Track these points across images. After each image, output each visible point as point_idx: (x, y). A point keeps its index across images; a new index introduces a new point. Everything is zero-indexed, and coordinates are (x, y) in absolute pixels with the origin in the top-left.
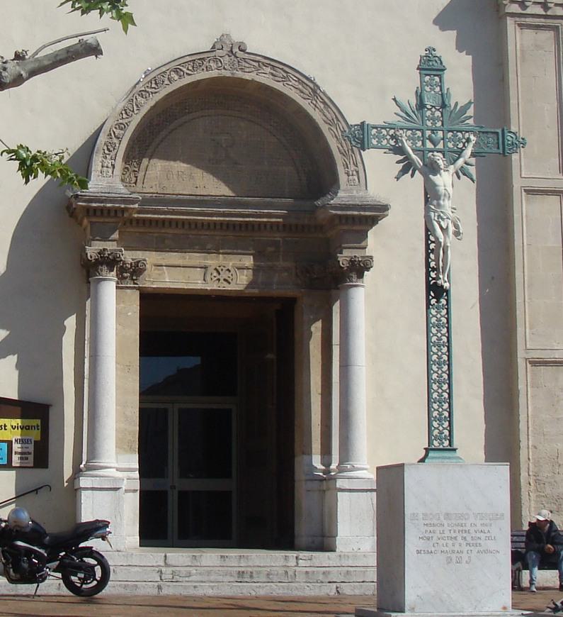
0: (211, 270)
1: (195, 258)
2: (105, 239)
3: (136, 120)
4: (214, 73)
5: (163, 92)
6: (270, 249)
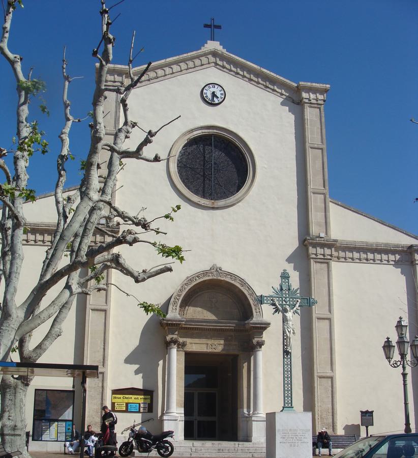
0: (209, 345)
1: (204, 341)
2: (173, 334)
3: (184, 293)
4: (211, 278)
5: (194, 284)
6: (230, 338)
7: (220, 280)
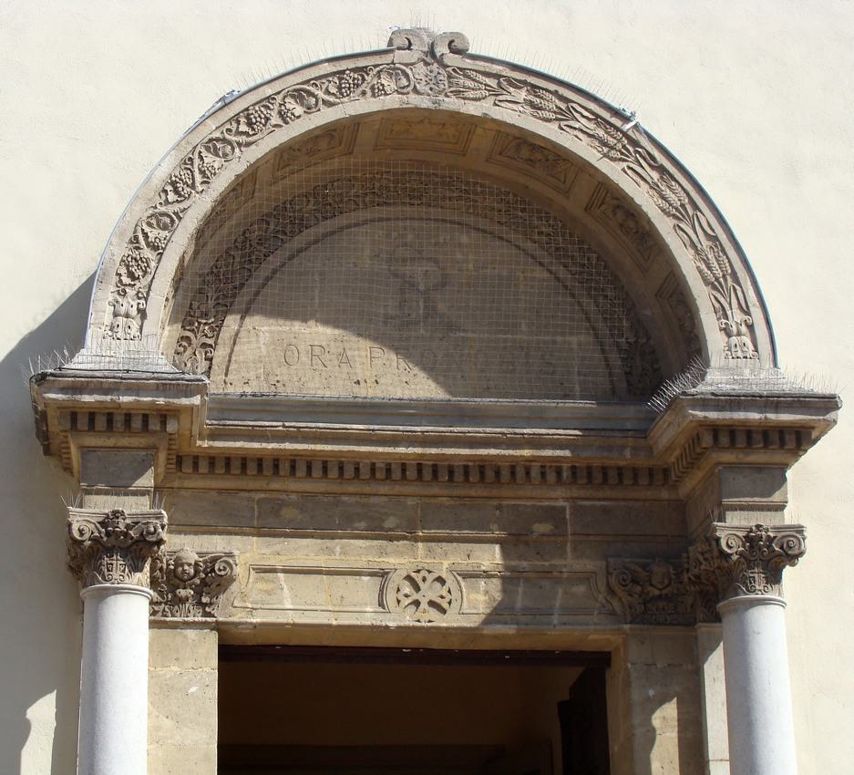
0: (396, 579)
1: (360, 552)
2: (120, 488)
3: (200, 205)
4: (392, 102)
5: (268, 142)
6: (541, 528)
7: (455, 115)
